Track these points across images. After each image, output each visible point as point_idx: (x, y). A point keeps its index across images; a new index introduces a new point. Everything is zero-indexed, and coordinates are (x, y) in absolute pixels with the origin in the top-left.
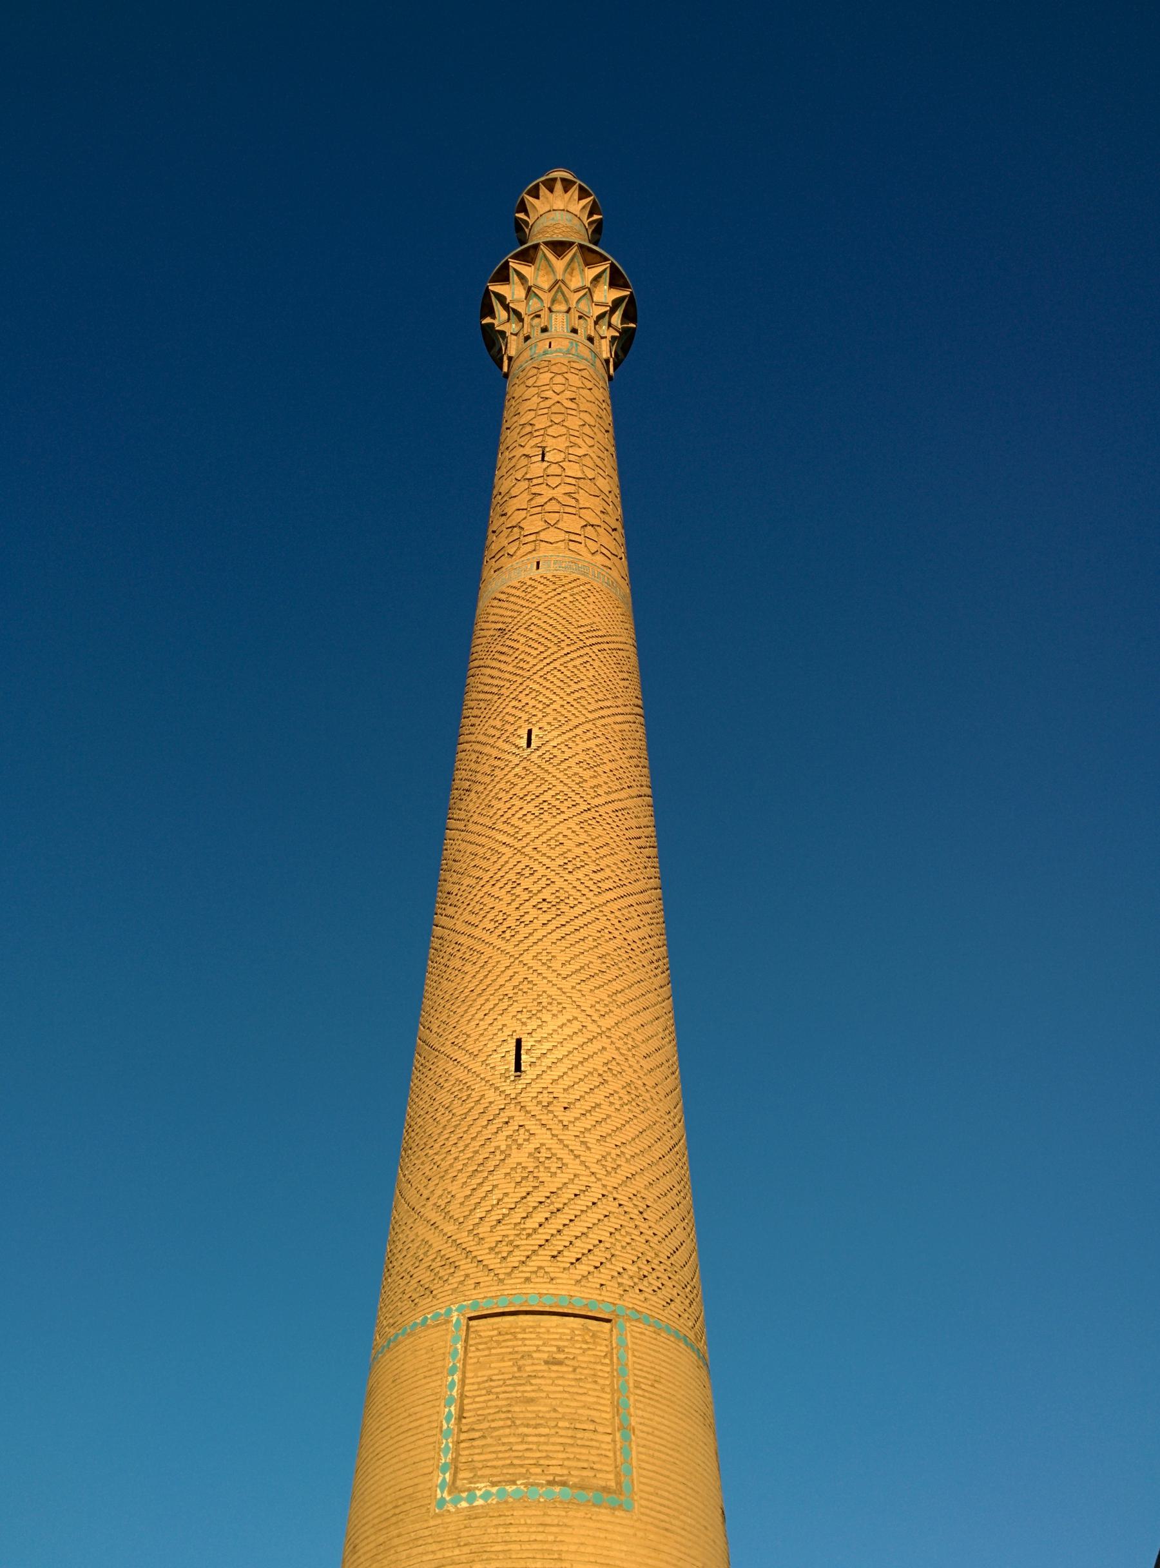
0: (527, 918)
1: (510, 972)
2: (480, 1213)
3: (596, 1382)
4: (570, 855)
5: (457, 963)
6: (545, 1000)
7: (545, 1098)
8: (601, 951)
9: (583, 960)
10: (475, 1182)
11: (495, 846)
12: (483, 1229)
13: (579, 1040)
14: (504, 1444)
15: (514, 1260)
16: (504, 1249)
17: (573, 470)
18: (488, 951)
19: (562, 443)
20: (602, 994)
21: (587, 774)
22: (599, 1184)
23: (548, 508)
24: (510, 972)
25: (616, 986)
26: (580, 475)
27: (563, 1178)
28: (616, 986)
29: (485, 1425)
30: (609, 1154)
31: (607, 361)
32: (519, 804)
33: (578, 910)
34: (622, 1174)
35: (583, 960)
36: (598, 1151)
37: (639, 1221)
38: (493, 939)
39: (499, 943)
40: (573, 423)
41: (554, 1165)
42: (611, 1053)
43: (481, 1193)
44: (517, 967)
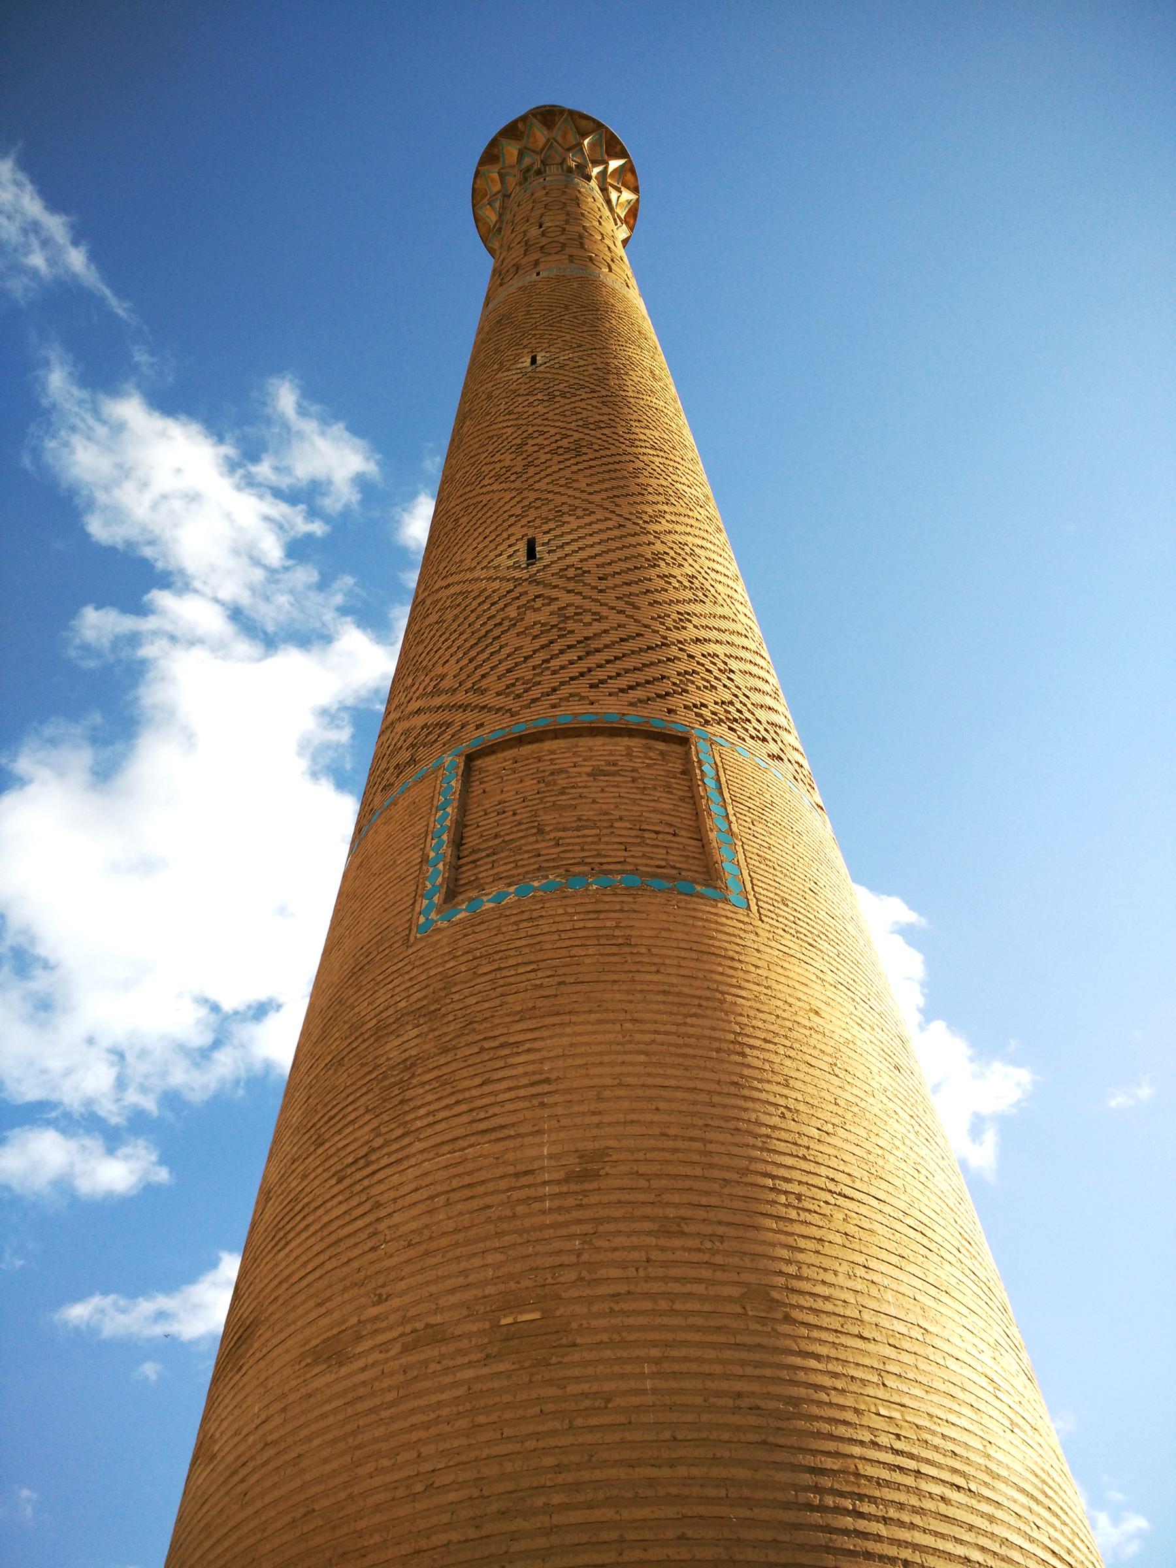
3: (671, 793)
6: (565, 509)
13: (617, 533)
14: (527, 852)
27: (597, 627)
38: (495, 487)
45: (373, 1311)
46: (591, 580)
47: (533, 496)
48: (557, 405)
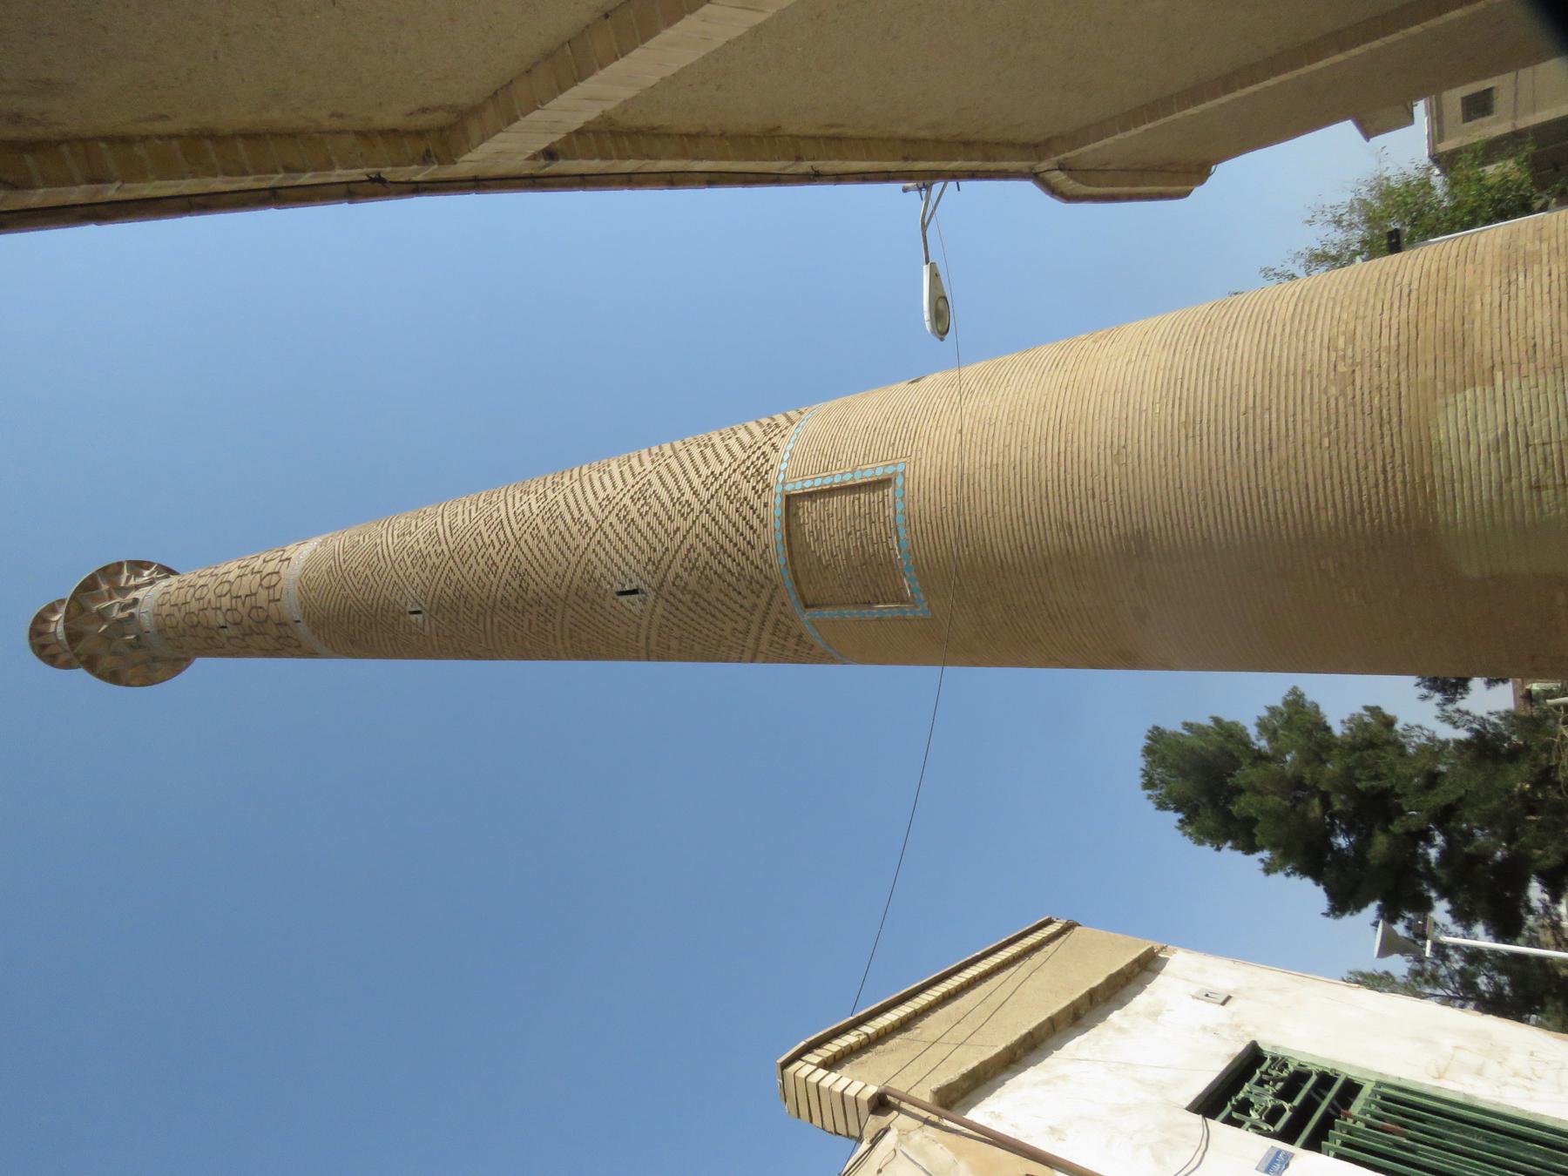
2: (736, 607)
6: (587, 577)
7: (650, 567)
12: (746, 604)
25: (568, 517)
32: (461, 616)
34: (693, 500)
36: (679, 521)
39: (559, 617)
41: (693, 555)
43: (724, 609)
44: (570, 601)
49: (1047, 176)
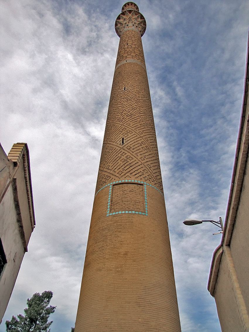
0: (124, 118)
1: (121, 127)
3: (140, 195)
4: (133, 107)
5: (110, 128)
6: (128, 131)
7: (129, 147)
8: (140, 123)
9: (136, 125)
10: (114, 163)
11: (118, 107)
12: (116, 170)
13: (136, 138)
15: (122, 175)
16: (120, 173)
17: (134, 46)
18: (116, 124)
19: (131, 42)
20: (141, 130)
21: (137, 94)
22: (140, 162)
23: (128, 52)
24: (121, 127)
25: (143, 130)
26: (135, 47)
28: (143, 130)
29: (117, 202)
30: (142, 157)
31: (140, 31)
33: (135, 116)
34: (145, 161)
35: (136, 125)
36: (140, 157)
37: (149, 169)
38: (117, 122)
39: (119, 123)
40: (133, 39)
41: (131, 159)
42: (142, 140)
43: (115, 164)
44: (122, 126)
45: (104, 266)
46: (131, 149)
47: (124, 127)
48: (128, 103)
49: (222, 248)
